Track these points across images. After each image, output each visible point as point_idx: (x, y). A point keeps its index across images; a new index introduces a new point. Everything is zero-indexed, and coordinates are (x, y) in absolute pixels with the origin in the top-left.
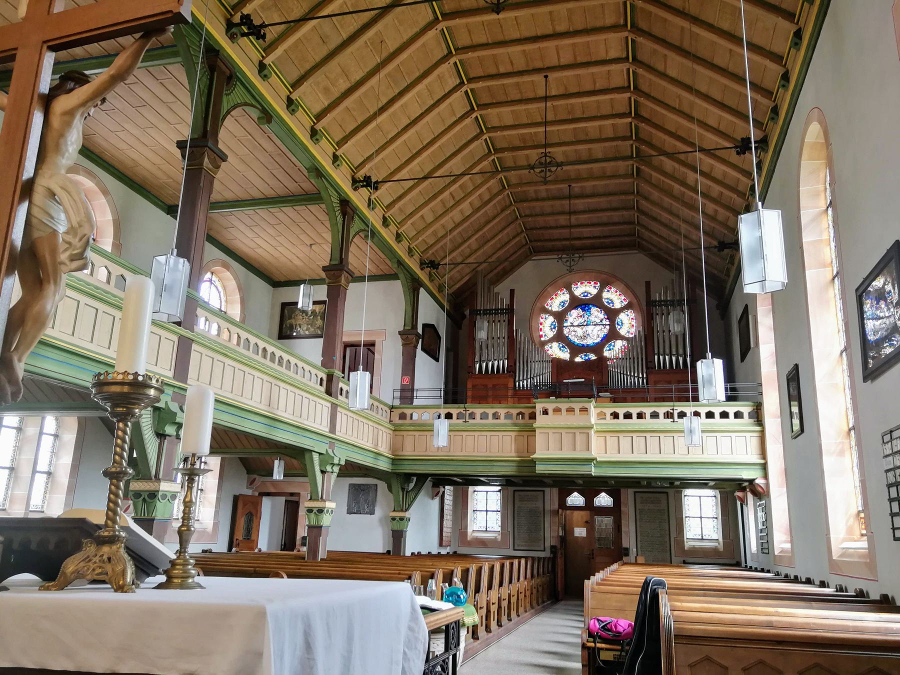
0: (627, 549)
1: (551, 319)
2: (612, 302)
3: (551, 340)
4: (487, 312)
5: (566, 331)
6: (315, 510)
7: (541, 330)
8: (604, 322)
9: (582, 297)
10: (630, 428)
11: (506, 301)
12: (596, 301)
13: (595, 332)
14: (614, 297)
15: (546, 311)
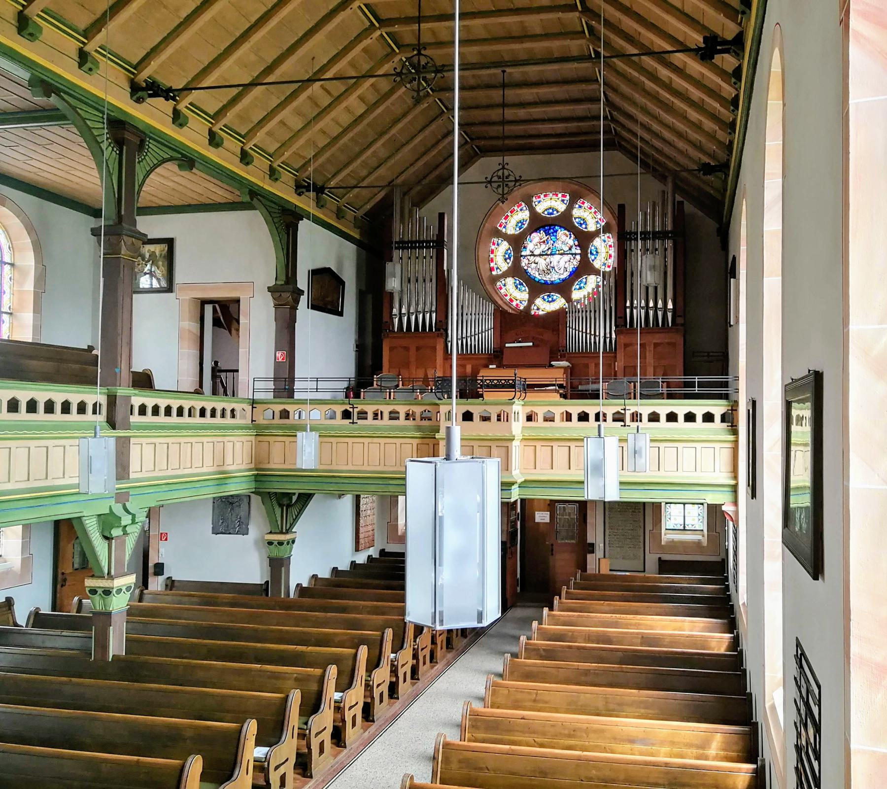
0: (592, 545)
1: (505, 245)
2: (585, 222)
3: (505, 275)
4: (403, 245)
5: (524, 263)
6: (100, 591)
7: (492, 261)
8: (573, 251)
9: (546, 214)
10: (566, 435)
11: (433, 231)
12: (565, 221)
13: (562, 264)
14: (589, 216)
15: (498, 234)
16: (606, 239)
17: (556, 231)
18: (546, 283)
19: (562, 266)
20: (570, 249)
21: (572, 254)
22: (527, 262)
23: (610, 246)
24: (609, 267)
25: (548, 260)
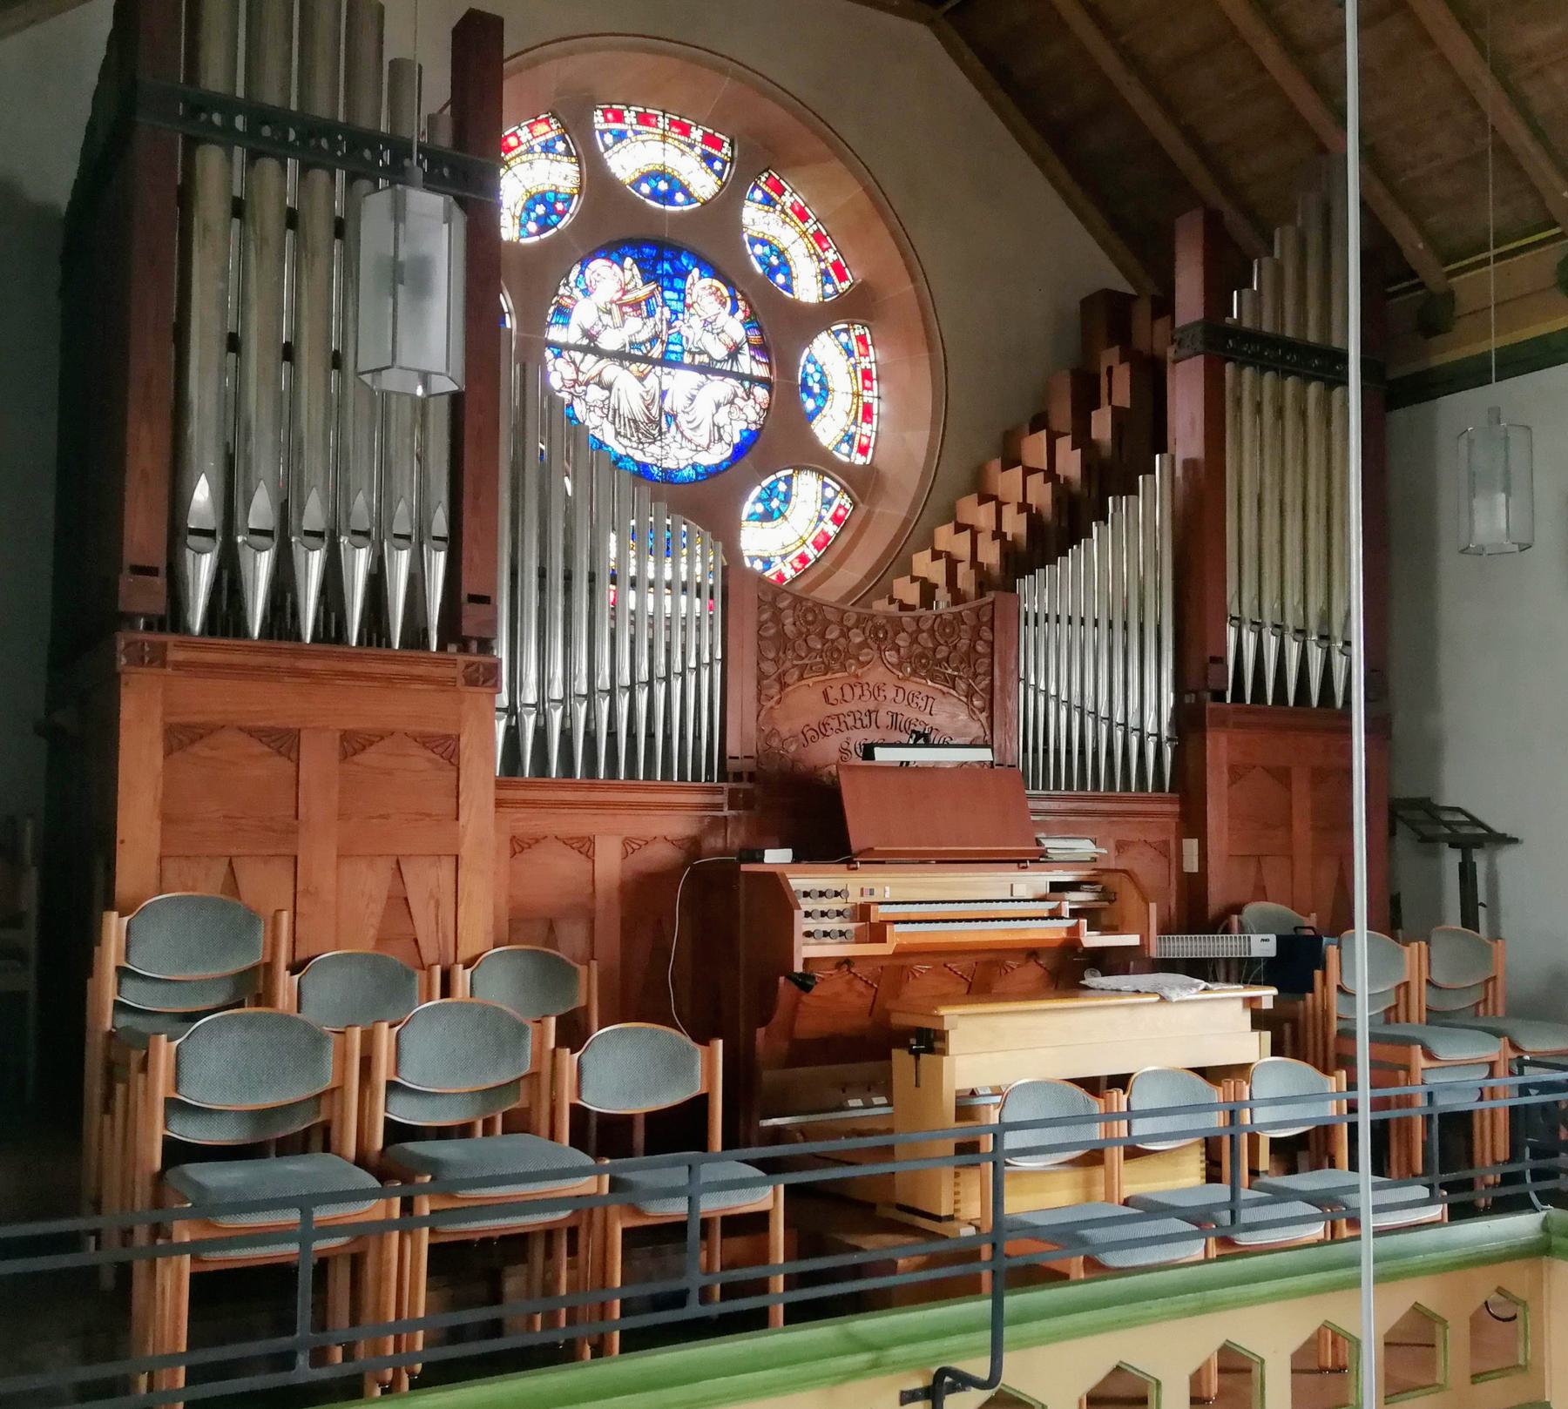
2: (785, 265)
13: (703, 410)
16: (854, 344)
17: (683, 274)
18: (643, 471)
19: (706, 419)
20: (734, 352)
21: (741, 377)
22: (569, 373)
23: (867, 375)
24: (863, 450)
25: (651, 382)
